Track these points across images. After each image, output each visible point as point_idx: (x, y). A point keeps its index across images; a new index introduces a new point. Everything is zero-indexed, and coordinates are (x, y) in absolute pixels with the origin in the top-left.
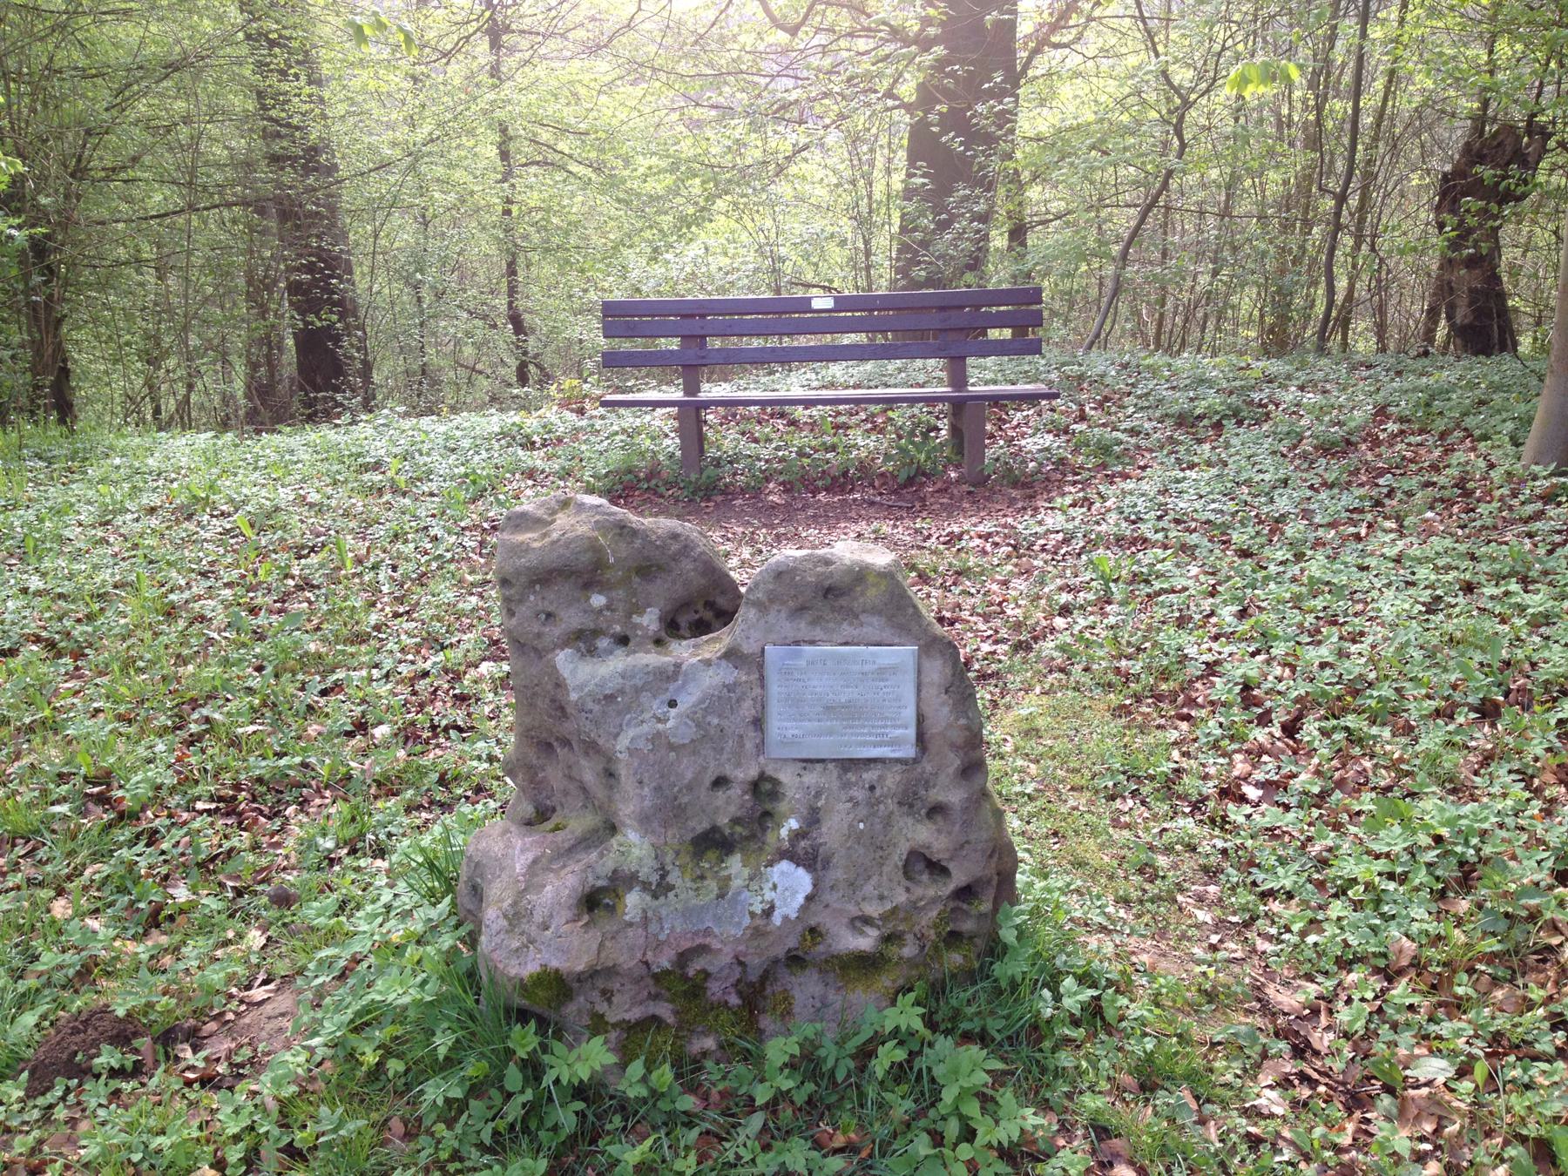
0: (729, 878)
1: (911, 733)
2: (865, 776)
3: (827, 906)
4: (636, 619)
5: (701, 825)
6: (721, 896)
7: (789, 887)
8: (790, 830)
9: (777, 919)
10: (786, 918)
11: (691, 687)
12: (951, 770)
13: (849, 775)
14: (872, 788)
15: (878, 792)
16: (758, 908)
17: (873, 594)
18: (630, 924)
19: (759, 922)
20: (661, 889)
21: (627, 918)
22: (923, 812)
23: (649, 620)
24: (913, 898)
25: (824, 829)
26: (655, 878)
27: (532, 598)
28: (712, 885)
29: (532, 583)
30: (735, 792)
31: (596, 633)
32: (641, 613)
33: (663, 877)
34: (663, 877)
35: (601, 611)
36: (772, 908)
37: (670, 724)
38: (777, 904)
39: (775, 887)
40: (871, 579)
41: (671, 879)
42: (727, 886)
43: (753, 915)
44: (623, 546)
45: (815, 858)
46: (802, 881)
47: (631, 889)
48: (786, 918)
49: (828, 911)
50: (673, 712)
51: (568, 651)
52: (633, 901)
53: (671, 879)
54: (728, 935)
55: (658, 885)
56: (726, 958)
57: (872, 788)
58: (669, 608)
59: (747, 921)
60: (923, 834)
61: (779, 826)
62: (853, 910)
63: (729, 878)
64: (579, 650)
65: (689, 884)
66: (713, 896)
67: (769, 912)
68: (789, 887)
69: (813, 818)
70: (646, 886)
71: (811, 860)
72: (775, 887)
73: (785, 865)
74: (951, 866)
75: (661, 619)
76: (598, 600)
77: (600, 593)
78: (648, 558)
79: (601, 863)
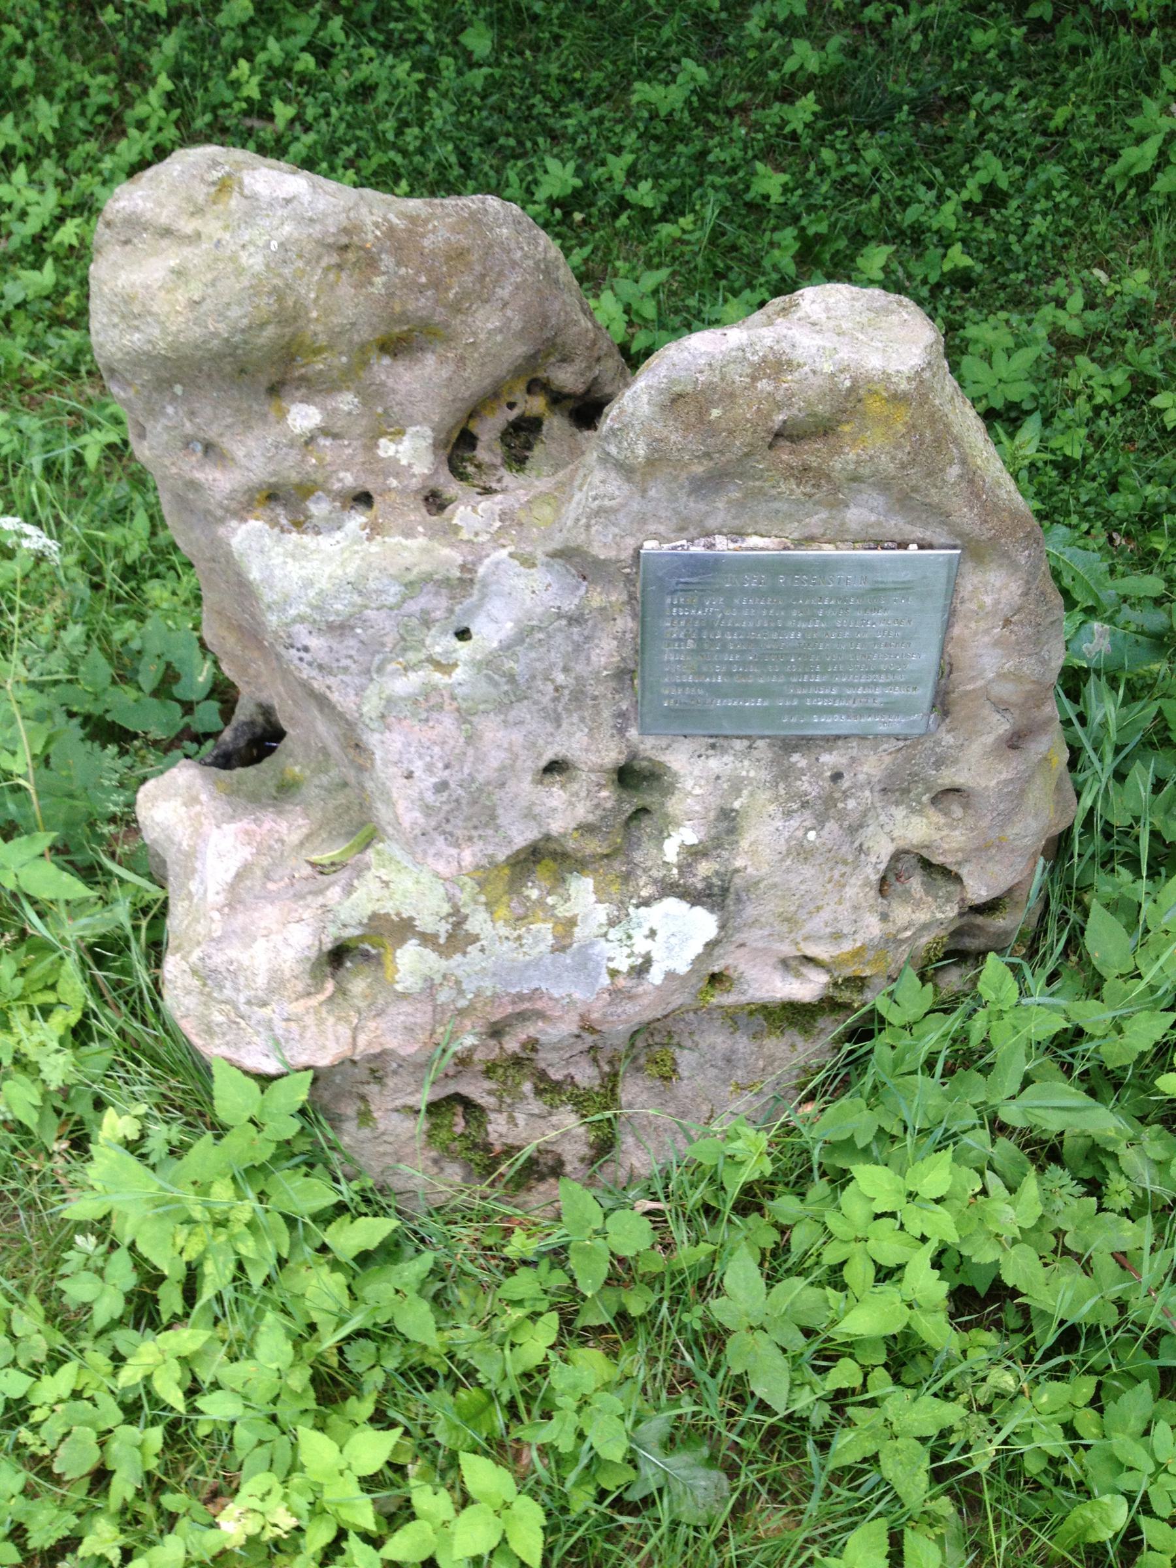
0: (572, 922)
1: (924, 693)
2: (826, 758)
3: (742, 945)
4: (386, 448)
5: (522, 836)
6: (560, 948)
7: (678, 934)
8: (682, 845)
9: (656, 976)
10: (670, 975)
11: (496, 606)
12: (989, 739)
13: (795, 757)
14: (837, 777)
15: (845, 783)
16: (623, 965)
17: (866, 447)
18: (404, 996)
19: (621, 982)
20: (457, 939)
21: (399, 988)
22: (925, 798)
23: (412, 453)
24: (891, 928)
25: (744, 844)
26: (444, 928)
27: (170, 410)
28: (544, 930)
29: (163, 384)
30: (584, 780)
31: (305, 490)
32: (398, 434)
33: (458, 925)
34: (458, 925)
35: (310, 441)
36: (648, 961)
37: (459, 674)
38: (655, 955)
39: (653, 933)
40: (874, 406)
41: (472, 926)
42: (569, 934)
43: (614, 973)
44: (345, 289)
45: (725, 890)
46: (702, 924)
47: (402, 941)
48: (670, 975)
49: (743, 950)
50: (464, 650)
51: (254, 525)
52: (409, 962)
53: (472, 926)
54: (572, 995)
55: (451, 937)
56: (568, 1027)
57: (837, 777)
58: (450, 421)
59: (605, 980)
60: (916, 828)
61: (660, 836)
62: (787, 949)
63: (572, 922)
64: (273, 522)
65: (505, 931)
66: (544, 947)
67: (641, 969)
68: (678, 934)
69: (727, 824)
70: (427, 939)
71: (714, 896)
72: (653, 933)
73: (672, 905)
74: (964, 872)
75: (436, 446)
76: (304, 417)
77: (305, 400)
78: (403, 318)
79: (353, 906)
